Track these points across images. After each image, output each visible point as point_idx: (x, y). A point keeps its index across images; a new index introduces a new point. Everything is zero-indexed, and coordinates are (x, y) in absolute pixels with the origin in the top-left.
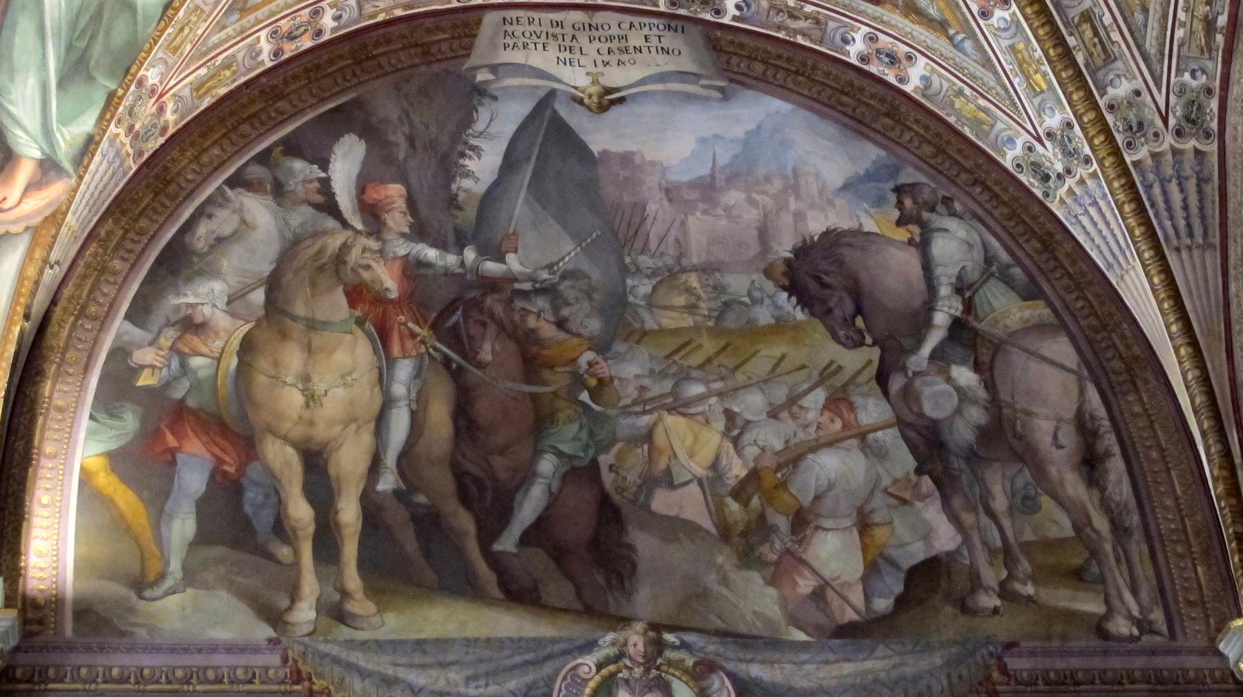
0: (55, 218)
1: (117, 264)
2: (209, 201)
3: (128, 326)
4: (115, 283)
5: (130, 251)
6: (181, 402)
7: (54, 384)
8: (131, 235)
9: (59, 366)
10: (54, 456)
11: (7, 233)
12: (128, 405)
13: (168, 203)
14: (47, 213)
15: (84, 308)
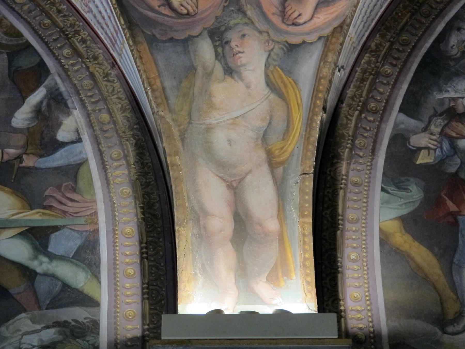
0: (341, 28)
1: (387, 69)
2: (456, 17)
3: (403, 117)
4: (388, 84)
5: (398, 59)
6: (456, 174)
7: (349, 164)
8: (396, 46)
9: (351, 150)
10: (356, 221)
11: (304, 42)
12: (412, 179)
13: (423, 20)
14: (336, 24)
15: (365, 104)
